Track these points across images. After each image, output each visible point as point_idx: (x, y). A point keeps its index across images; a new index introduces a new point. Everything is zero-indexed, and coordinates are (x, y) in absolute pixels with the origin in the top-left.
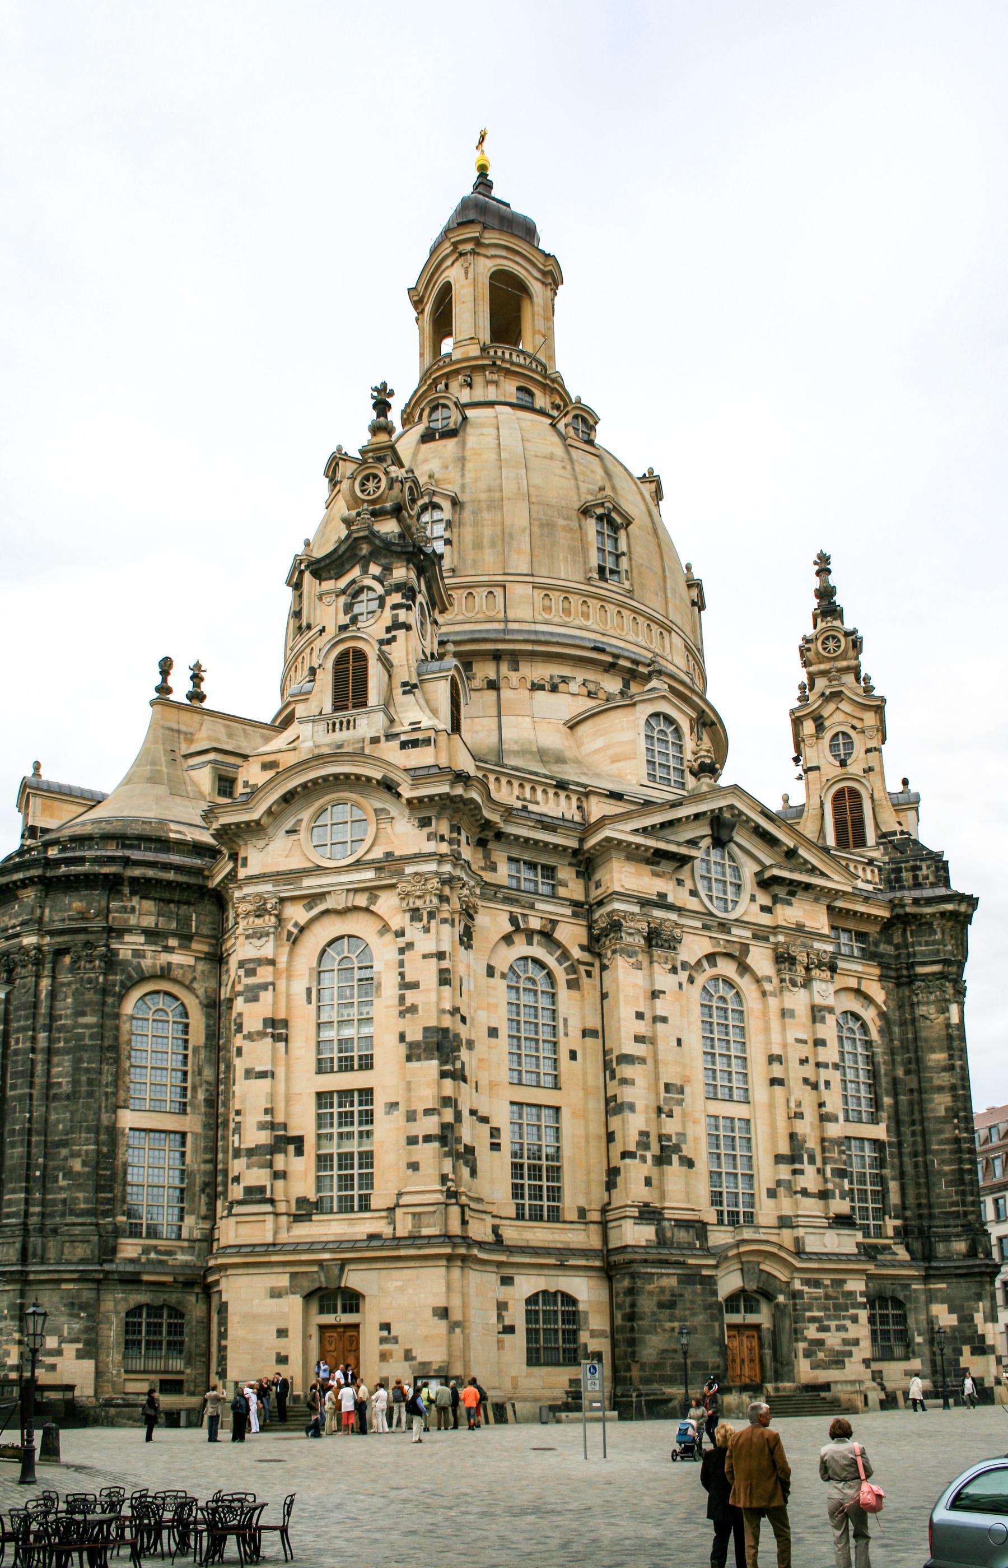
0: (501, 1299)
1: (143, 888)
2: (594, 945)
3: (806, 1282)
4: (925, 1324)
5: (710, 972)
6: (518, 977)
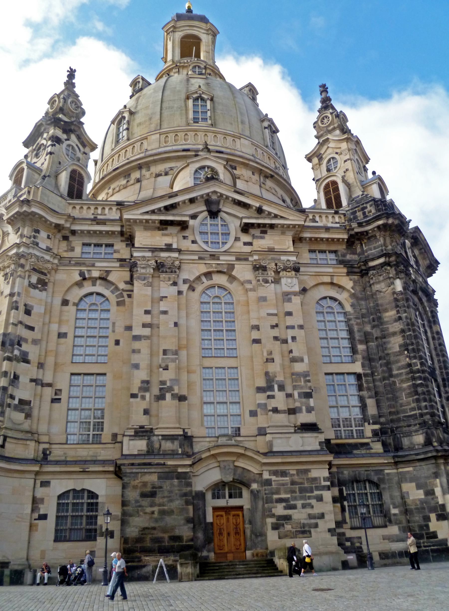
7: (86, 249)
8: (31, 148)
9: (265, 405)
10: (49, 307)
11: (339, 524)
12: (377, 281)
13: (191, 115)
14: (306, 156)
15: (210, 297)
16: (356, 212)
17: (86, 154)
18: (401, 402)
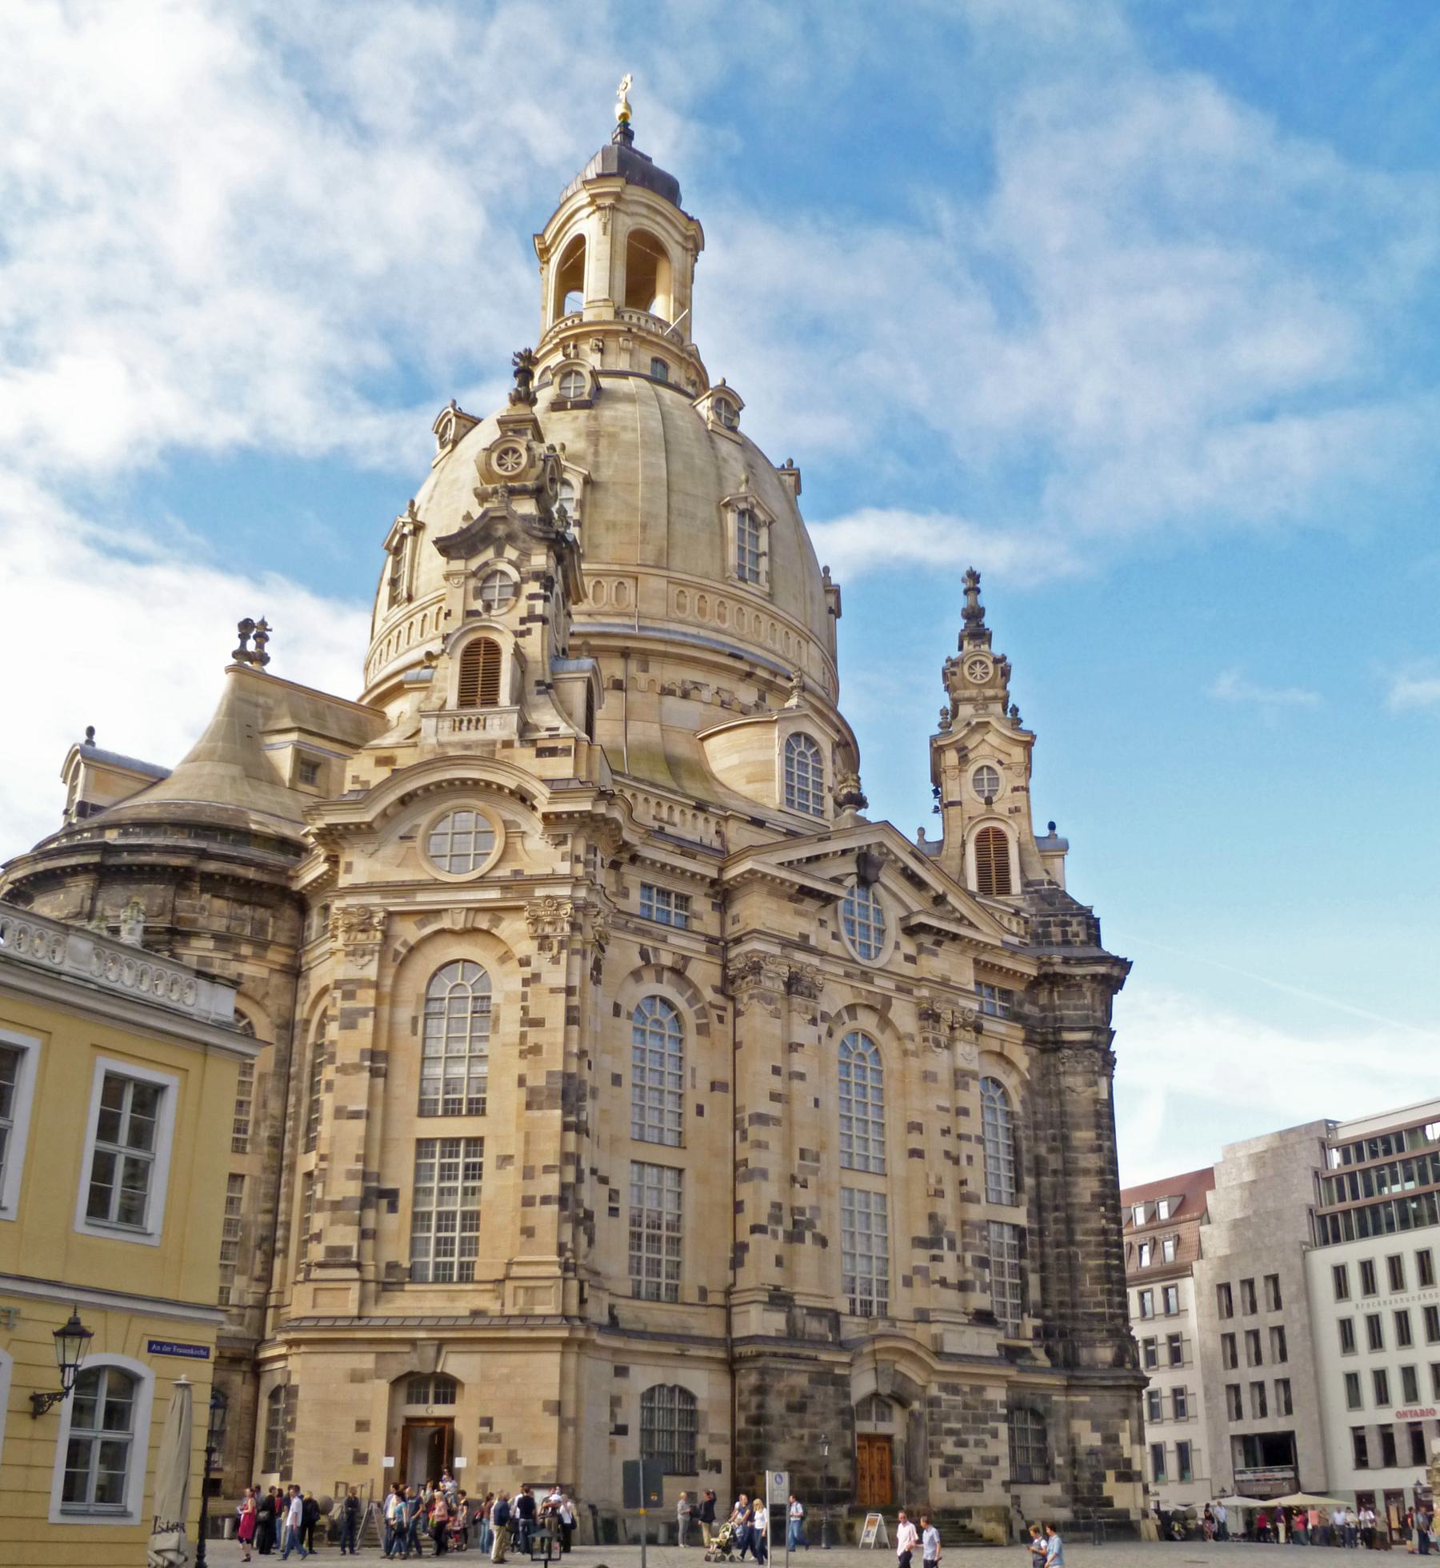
0: (615, 1392)
1: (214, 884)
2: (727, 986)
3: (945, 1388)
5: (850, 1025)
6: (645, 1018)
8: (458, 565)
13: (732, 558)
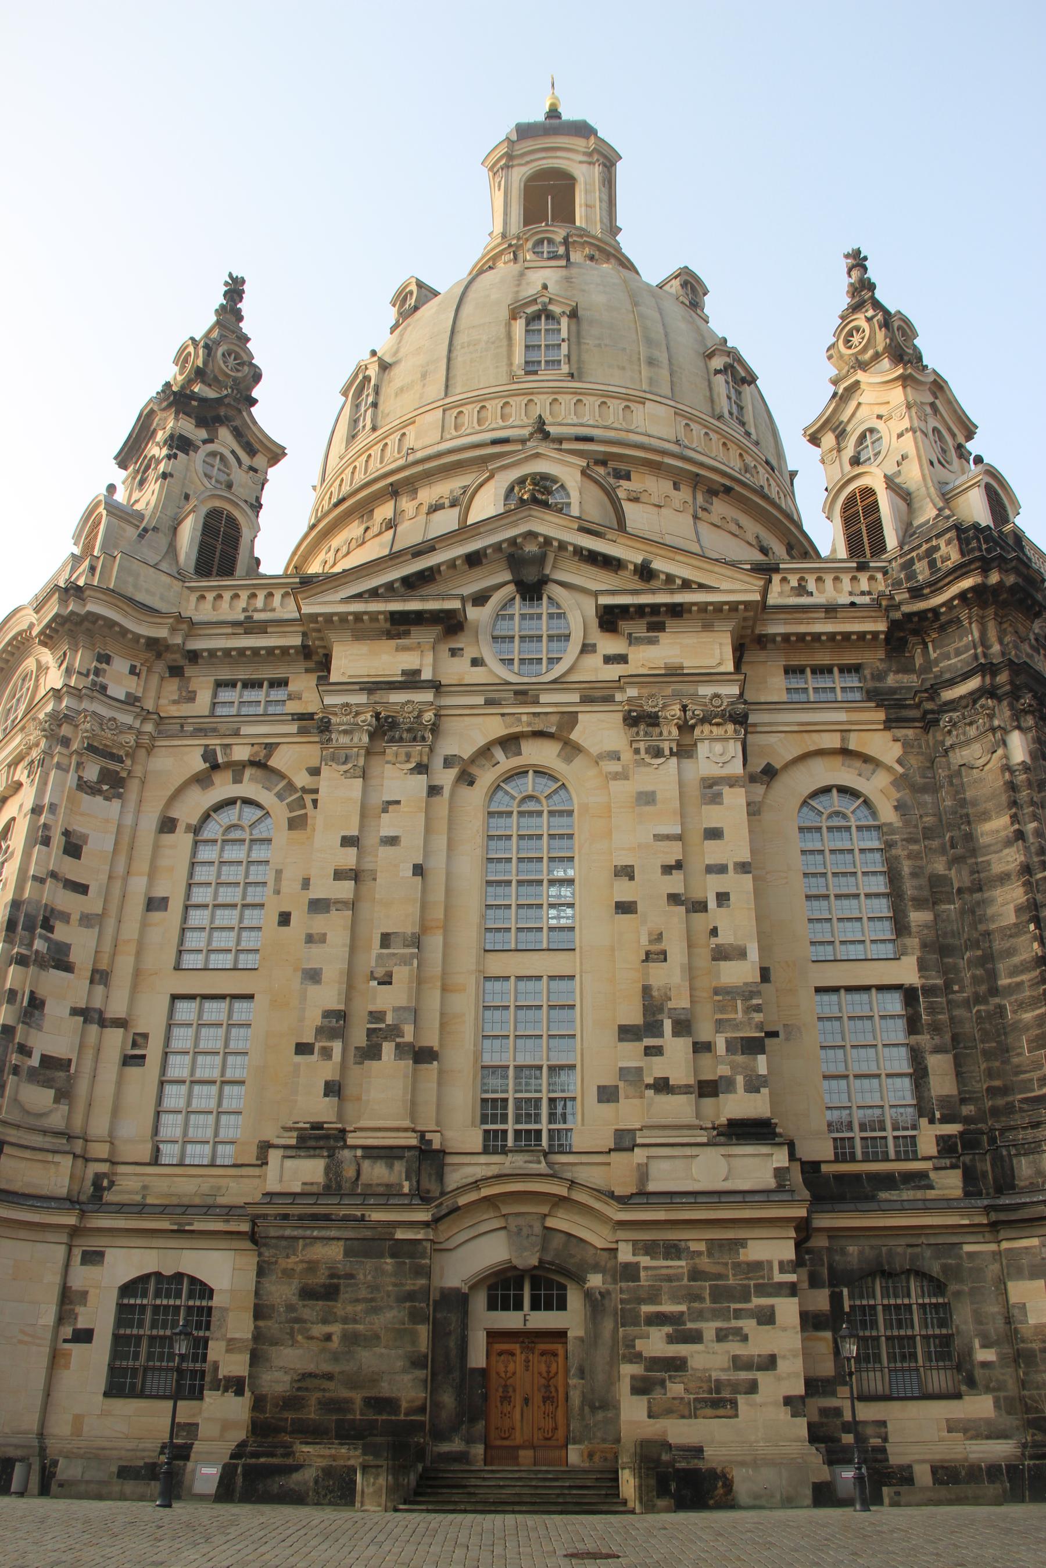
3: (639, 1247)
4: (1000, 1322)
7: (225, 695)
9: (639, 1070)
10: (126, 839)
11: (814, 1386)
12: (962, 738)
13: (519, 357)
14: (805, 430)
15: (513, 798)
16: (911, 562)
17: (255, 471)
18: (1016, 1060)
